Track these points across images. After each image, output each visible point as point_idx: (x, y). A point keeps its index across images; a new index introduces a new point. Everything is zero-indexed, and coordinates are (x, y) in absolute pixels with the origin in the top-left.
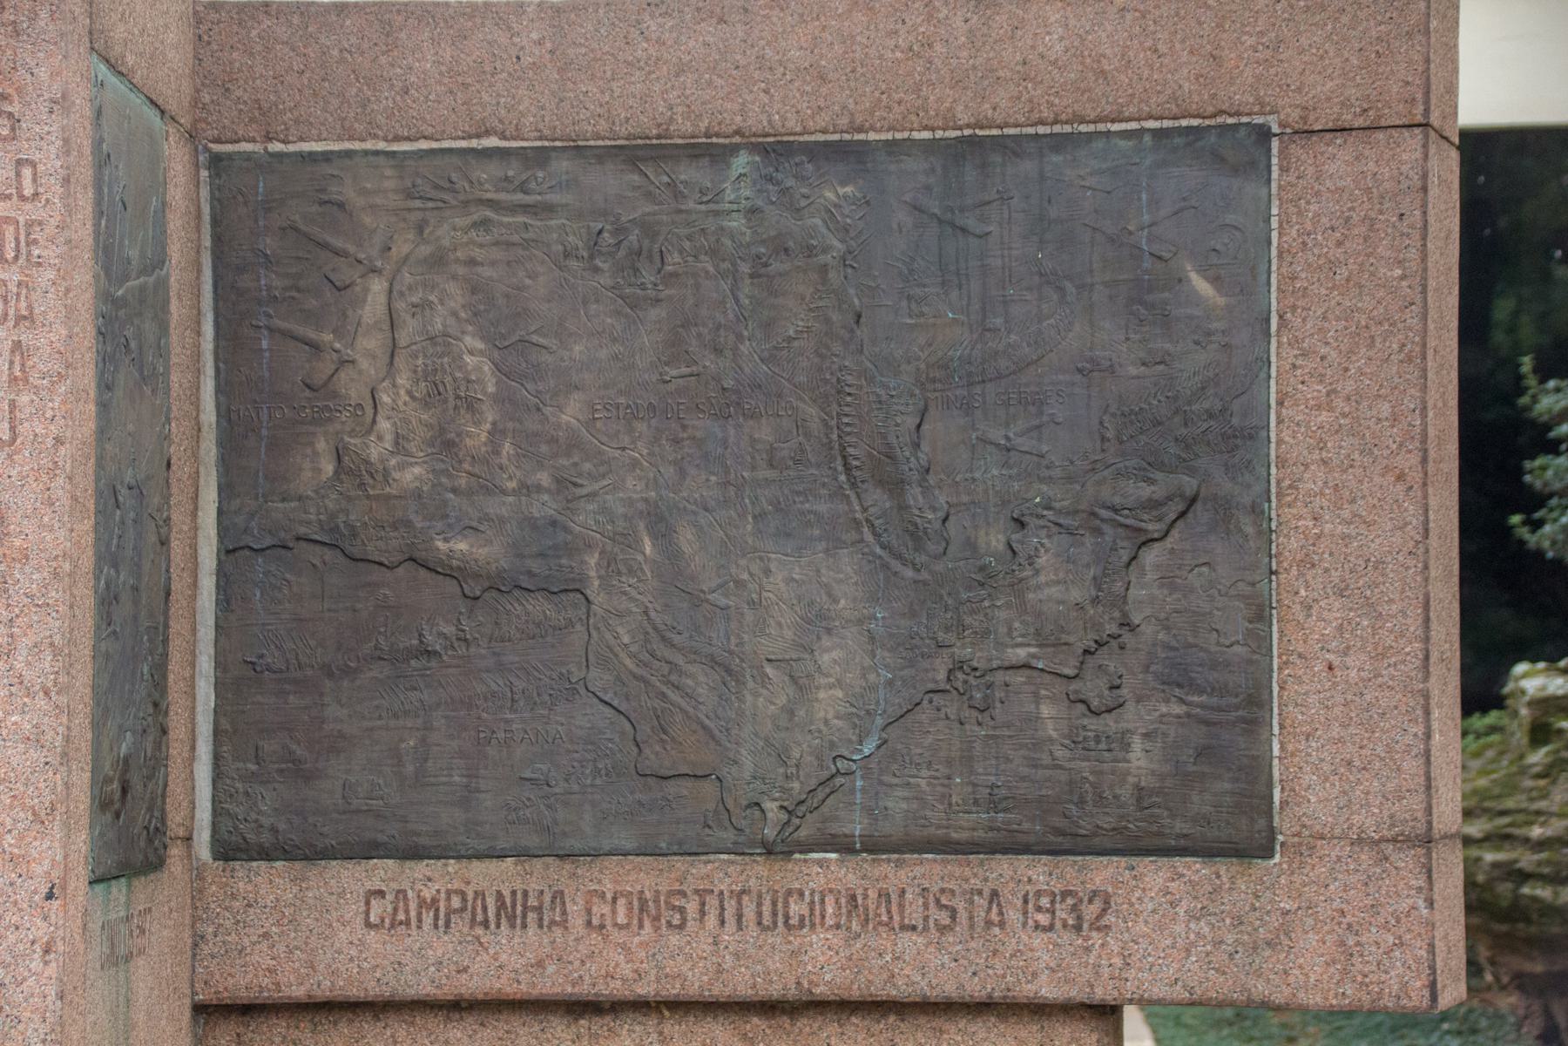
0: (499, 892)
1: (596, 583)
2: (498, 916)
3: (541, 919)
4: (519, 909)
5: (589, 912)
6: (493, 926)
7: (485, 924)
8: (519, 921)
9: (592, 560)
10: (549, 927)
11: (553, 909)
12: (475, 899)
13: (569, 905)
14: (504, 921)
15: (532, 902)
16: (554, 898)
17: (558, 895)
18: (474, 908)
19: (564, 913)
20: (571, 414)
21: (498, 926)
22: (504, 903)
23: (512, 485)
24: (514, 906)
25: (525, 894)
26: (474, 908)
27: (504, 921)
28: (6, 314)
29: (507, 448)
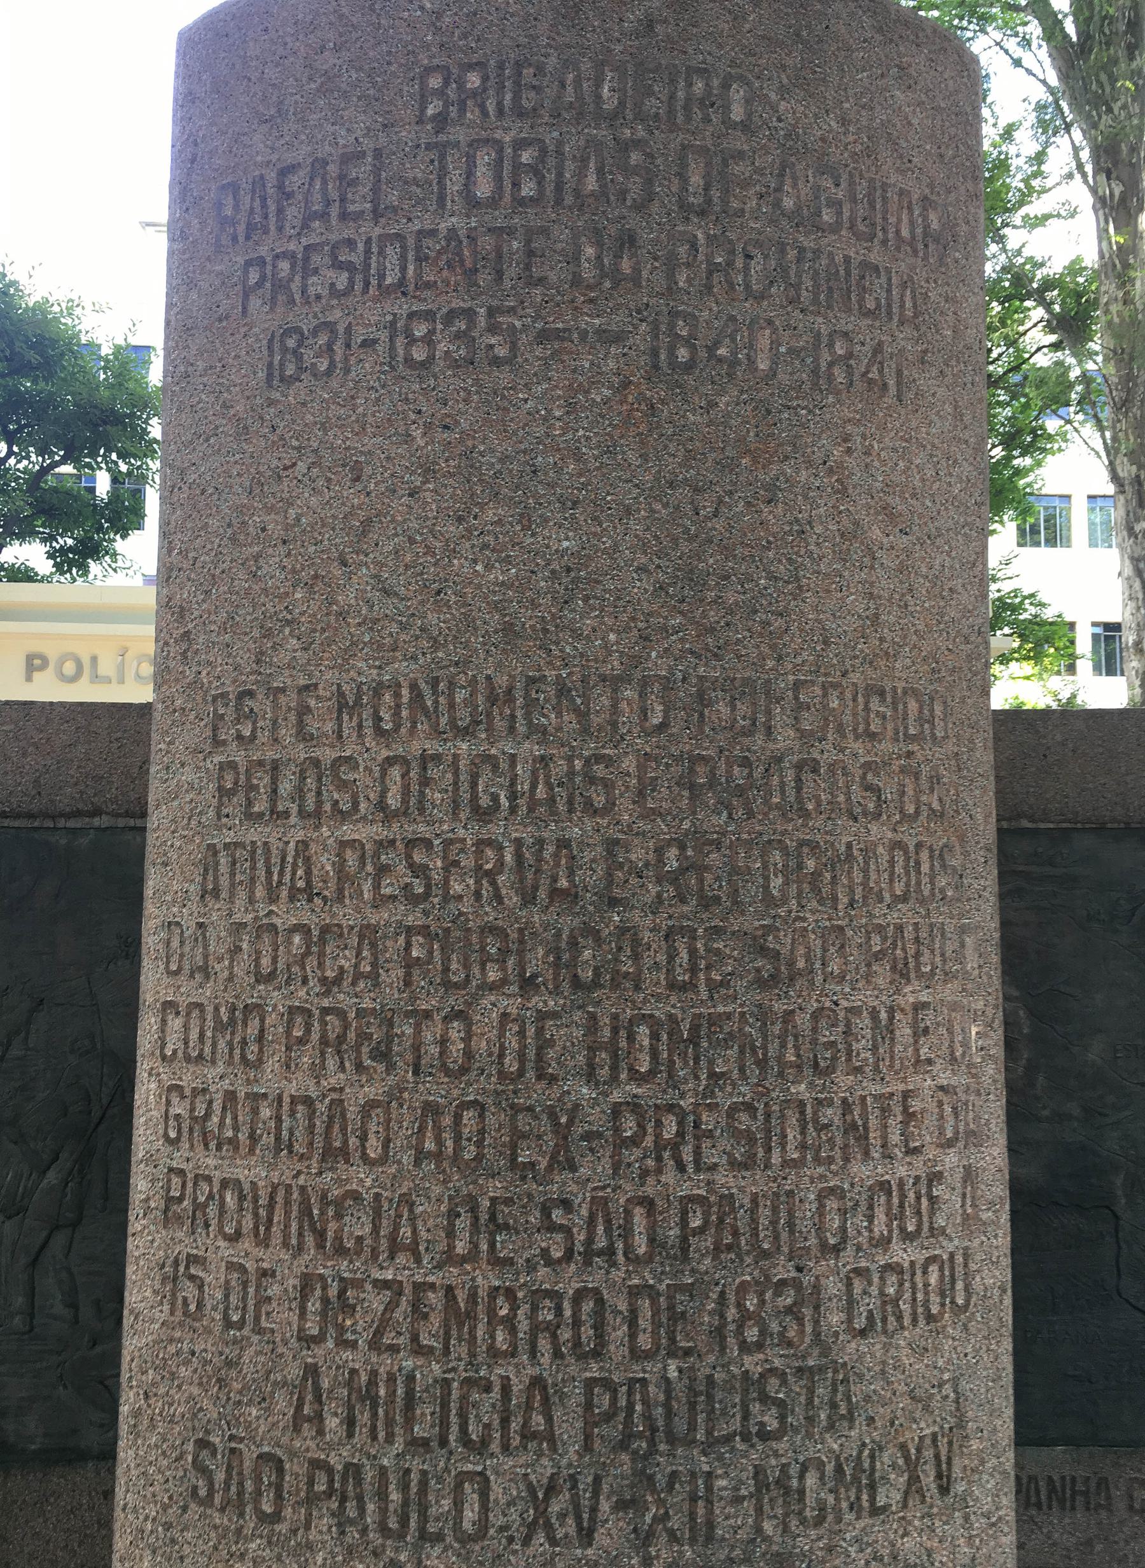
0: (1050, 1478)
1: (1123, 1201)
2: (1050, 1498)
3: (1088, 1503)
4: (1068, 1492)
5: (1131, 1497)
6: (1045, 1507)
7: (1039, 1506)
8: (1068, 1504)
9: (1119, 1181)
10: (1096, 1509)
11: (1099, 1494)
12: (1029, 1482)
13: (1112, 1491)
14: (1055, 1504)
15: (1079, 1487)
16: (1099, 1485)
17: (1103, 1483)
18: (1028, 1491)
19: (1109, 1498)
20: (1095, 1053)
21: (1050, 1508)
22: (1054, 1487)
23: (1046, 1113)
24: (1064, 1491)
25: (1073, 1479)
26: (1028, 1491)
27: (1055, 1504)
28: (958, 1132)
29: (1041, 1080)
